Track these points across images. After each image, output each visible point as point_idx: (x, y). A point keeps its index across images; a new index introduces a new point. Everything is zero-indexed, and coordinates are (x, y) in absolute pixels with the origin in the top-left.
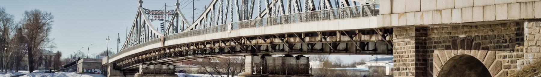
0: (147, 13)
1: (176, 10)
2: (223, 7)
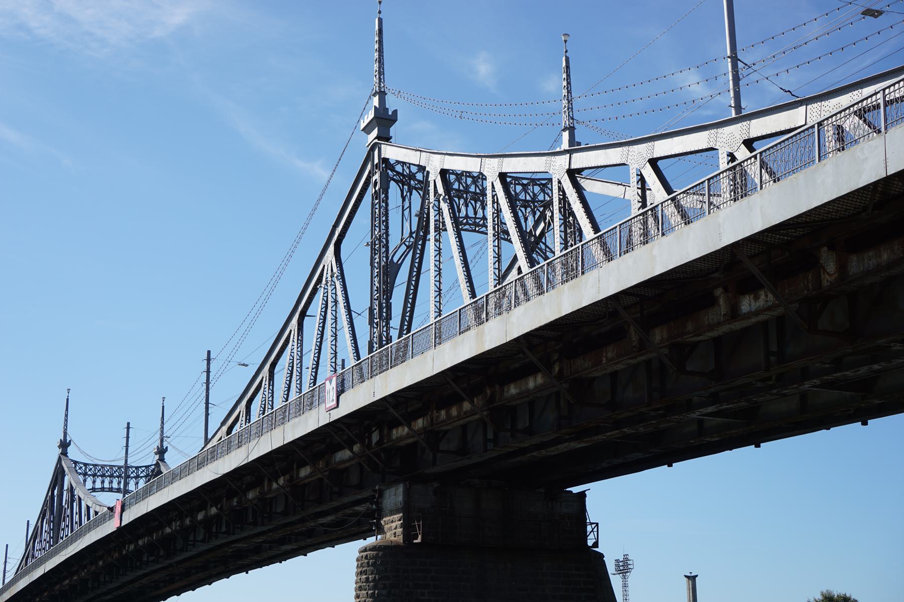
0: (79, 471)
1: (157, 465)
2: (301, 357)
